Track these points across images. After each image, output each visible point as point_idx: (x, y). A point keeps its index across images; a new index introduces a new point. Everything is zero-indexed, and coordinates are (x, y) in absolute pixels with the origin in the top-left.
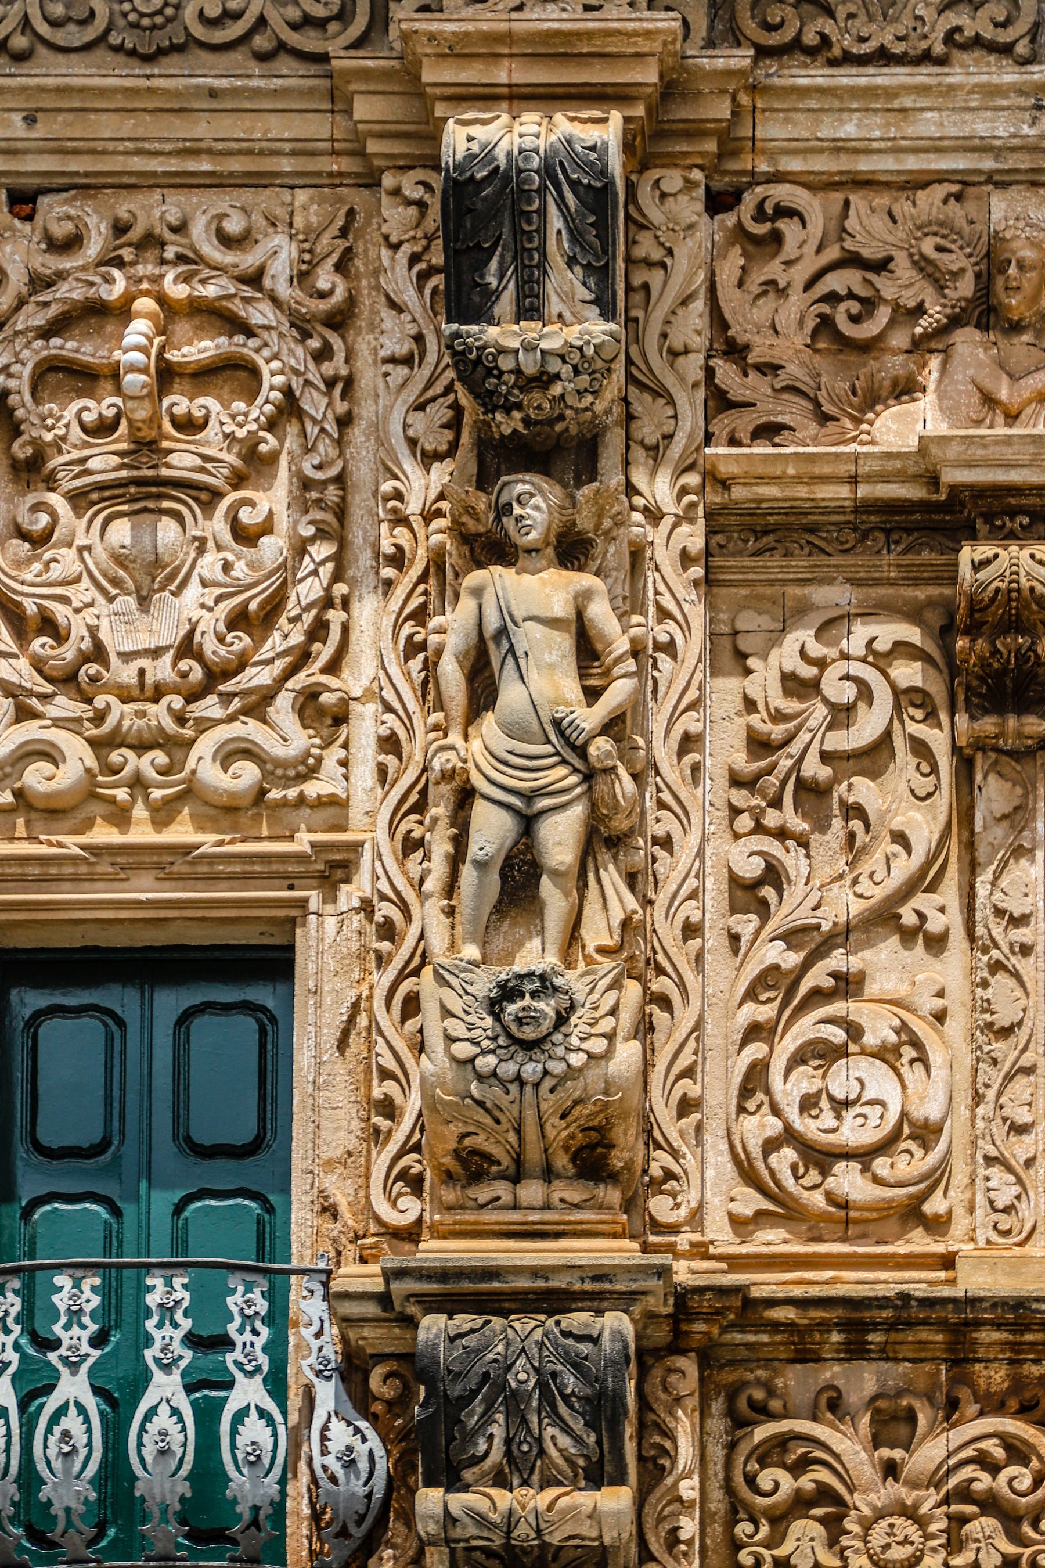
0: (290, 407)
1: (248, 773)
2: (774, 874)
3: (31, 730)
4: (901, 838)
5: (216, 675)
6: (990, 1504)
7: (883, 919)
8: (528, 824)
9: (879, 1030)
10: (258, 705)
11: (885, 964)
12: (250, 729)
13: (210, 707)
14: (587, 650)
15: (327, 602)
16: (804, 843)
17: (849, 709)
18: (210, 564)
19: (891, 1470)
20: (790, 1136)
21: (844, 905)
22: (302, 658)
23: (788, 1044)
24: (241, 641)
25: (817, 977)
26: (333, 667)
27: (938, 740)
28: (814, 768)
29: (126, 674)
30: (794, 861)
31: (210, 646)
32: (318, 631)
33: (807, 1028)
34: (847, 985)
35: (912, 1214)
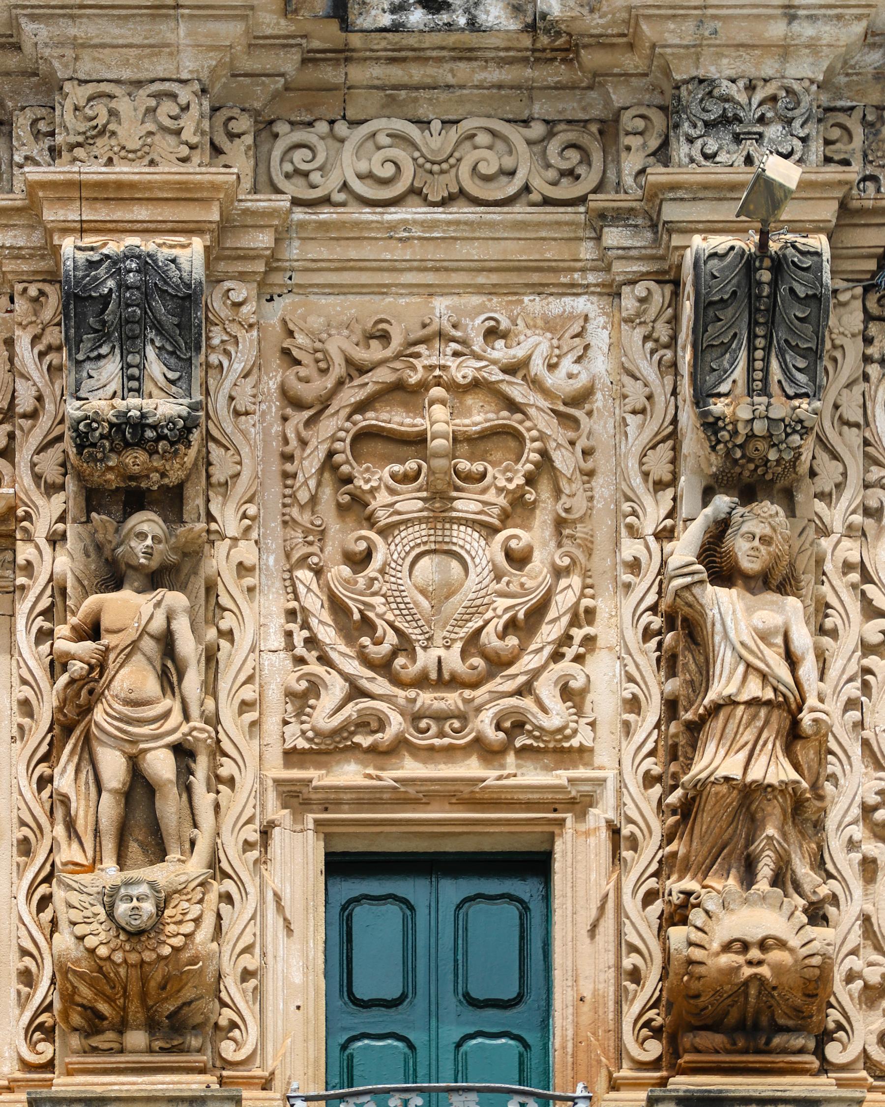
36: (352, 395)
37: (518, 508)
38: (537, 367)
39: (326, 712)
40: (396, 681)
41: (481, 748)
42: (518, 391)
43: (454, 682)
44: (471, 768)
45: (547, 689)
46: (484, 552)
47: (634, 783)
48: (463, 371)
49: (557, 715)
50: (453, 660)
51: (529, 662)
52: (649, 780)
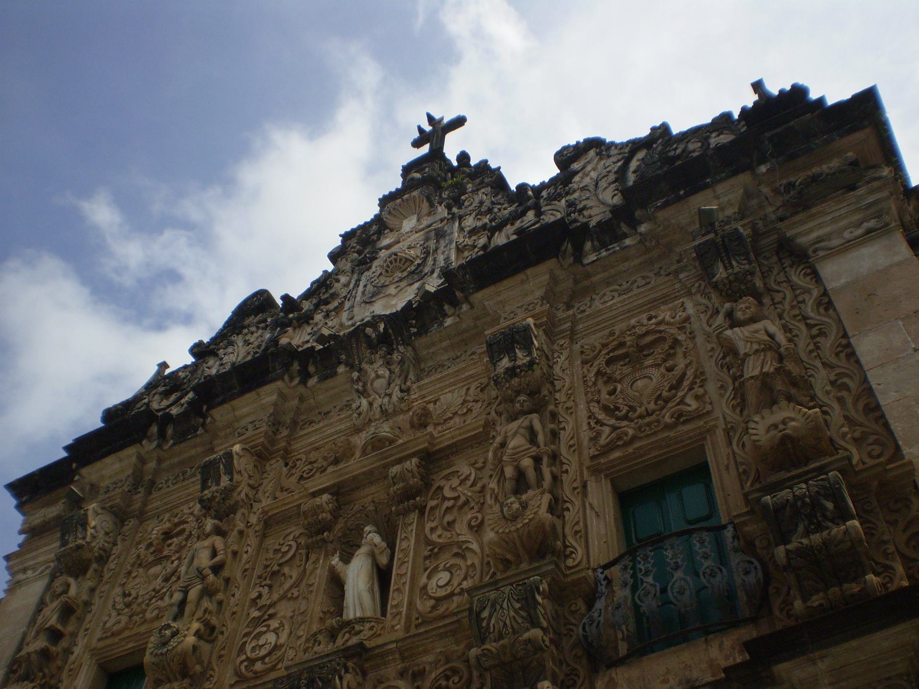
2: (260, 596)
4: (291, 577)
7: (283, 597)
11: (285, 609)
12: (160, 603)
14: (214, 553)
16: (270, 587)
21: (275, 596)
25: (266, 617)
28: (276, 568)
34: (271, 616)
36: (604, 352)
41: (667, 427)
45: (688, 400)
46: (656, 373)
49: (693, 405)
50: (652, 406)
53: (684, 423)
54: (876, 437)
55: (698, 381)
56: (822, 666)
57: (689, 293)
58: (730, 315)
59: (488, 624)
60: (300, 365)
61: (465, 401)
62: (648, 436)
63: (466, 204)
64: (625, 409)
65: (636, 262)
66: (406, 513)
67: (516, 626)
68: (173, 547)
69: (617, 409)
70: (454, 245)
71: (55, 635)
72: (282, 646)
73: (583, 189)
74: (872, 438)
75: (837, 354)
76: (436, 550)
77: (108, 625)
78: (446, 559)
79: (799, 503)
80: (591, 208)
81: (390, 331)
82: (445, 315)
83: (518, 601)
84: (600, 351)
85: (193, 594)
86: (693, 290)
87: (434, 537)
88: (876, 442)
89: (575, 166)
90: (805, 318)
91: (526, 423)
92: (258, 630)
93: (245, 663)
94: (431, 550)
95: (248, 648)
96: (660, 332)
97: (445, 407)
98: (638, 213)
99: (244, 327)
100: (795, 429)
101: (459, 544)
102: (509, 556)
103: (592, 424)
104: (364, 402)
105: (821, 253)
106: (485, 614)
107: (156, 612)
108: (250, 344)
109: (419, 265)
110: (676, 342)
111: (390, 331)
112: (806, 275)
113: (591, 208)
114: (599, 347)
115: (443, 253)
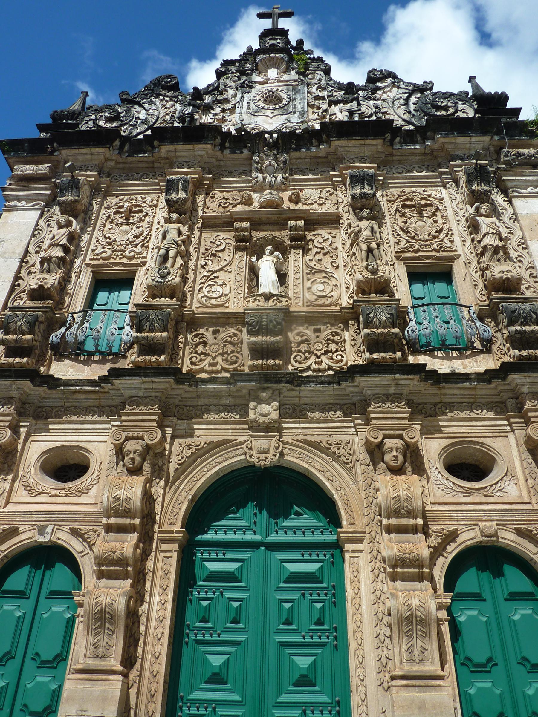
0: (147, 215)
1: (132, 254)
2: (206, 264)
3: (104, 250)
5: (131, 242)
6: (230, 343)
7: (221, 269)
8: (167, 252)
9: (220, 282)
10: (136, 246)
12: (134, 249)
13: (129, 246)
14: (180, 233)
15: (148, 235)
16: (211, 260)
17: (219, 245)
18: (133, 231)
19: (215, 338)
20: (205, 296)
21: (217, 268)
22: (143, 241)
23: (206, 285)
24: (135, 239)
25: (212, 277)
26: (148, 242)
27: (232, 248)
28: (214, 252)
29: (119, 244)
30: (210, 263)
31: (131, 240)
32: (146, 238)
33: (209, 283)
34: (216, 277)
35: (222, 305)
37: (434, 215)
38: (433, 195)
39: (403, 244)
40: (417, 240)
42: (431, 199)
43: (427, 240)
44: (434, 253)
45: (446, 240)
46: (430, 221)
47: (468, 254)
48: (421, 196)
49: (449, 244)
50: (426, 237)
51: (441, 236)
52: (471, 253)
53: (443, 251)
54: (534, 290)
55: (450, 233)
56: (528, 380)
57: (444, 186)
58: (477, 209)
59: (372, 320)
60: (221, 139)
61: (320, 197)
62: (424, 251)
63: (310, 77)
64: (413, 234)
65: (418, 158)
66: (295, 248)
67: (385, 325)
68: (136, 218)
69: (408, 232)
70: (306, 101)
71: (65, 249)
72: (226, 295)
73: (384, 100)
74: (533, 290)
75: (518, 246)
76: (313, 272)
77: (97, 252)
78: (319, 277)
79: (522, 312)
80: (390, 114)
81: (280, 141)
82: (312, 145)
83: (389, 314)
84: (397, 199)
85: (172, 253)
86: (448, 186)
87: (312, 264)
88: (535, 292)
89: (379, 84)
90: (504, 223)
91: (370, 225)
92: (209, 283)
93: (205, 298)
94: (311, 271)
95: (205, 290)
96: (430, 201)
97: (308, 196)
98: (429, 133)
99: (162, 96)
100: (512, 276)
101: (326, 272)
102: (366, 289)
103: (395, 234)
104: (260, 176)
105: (516, 194)
106: (371, 315)
107: (132, 254)
108: (166, 108)
109: (286, 105)
110: (438, 209)
111: (280, 141)
112: (504, 201)
113: (390, 114)
114: (396, 196)
115: (300, 103)
